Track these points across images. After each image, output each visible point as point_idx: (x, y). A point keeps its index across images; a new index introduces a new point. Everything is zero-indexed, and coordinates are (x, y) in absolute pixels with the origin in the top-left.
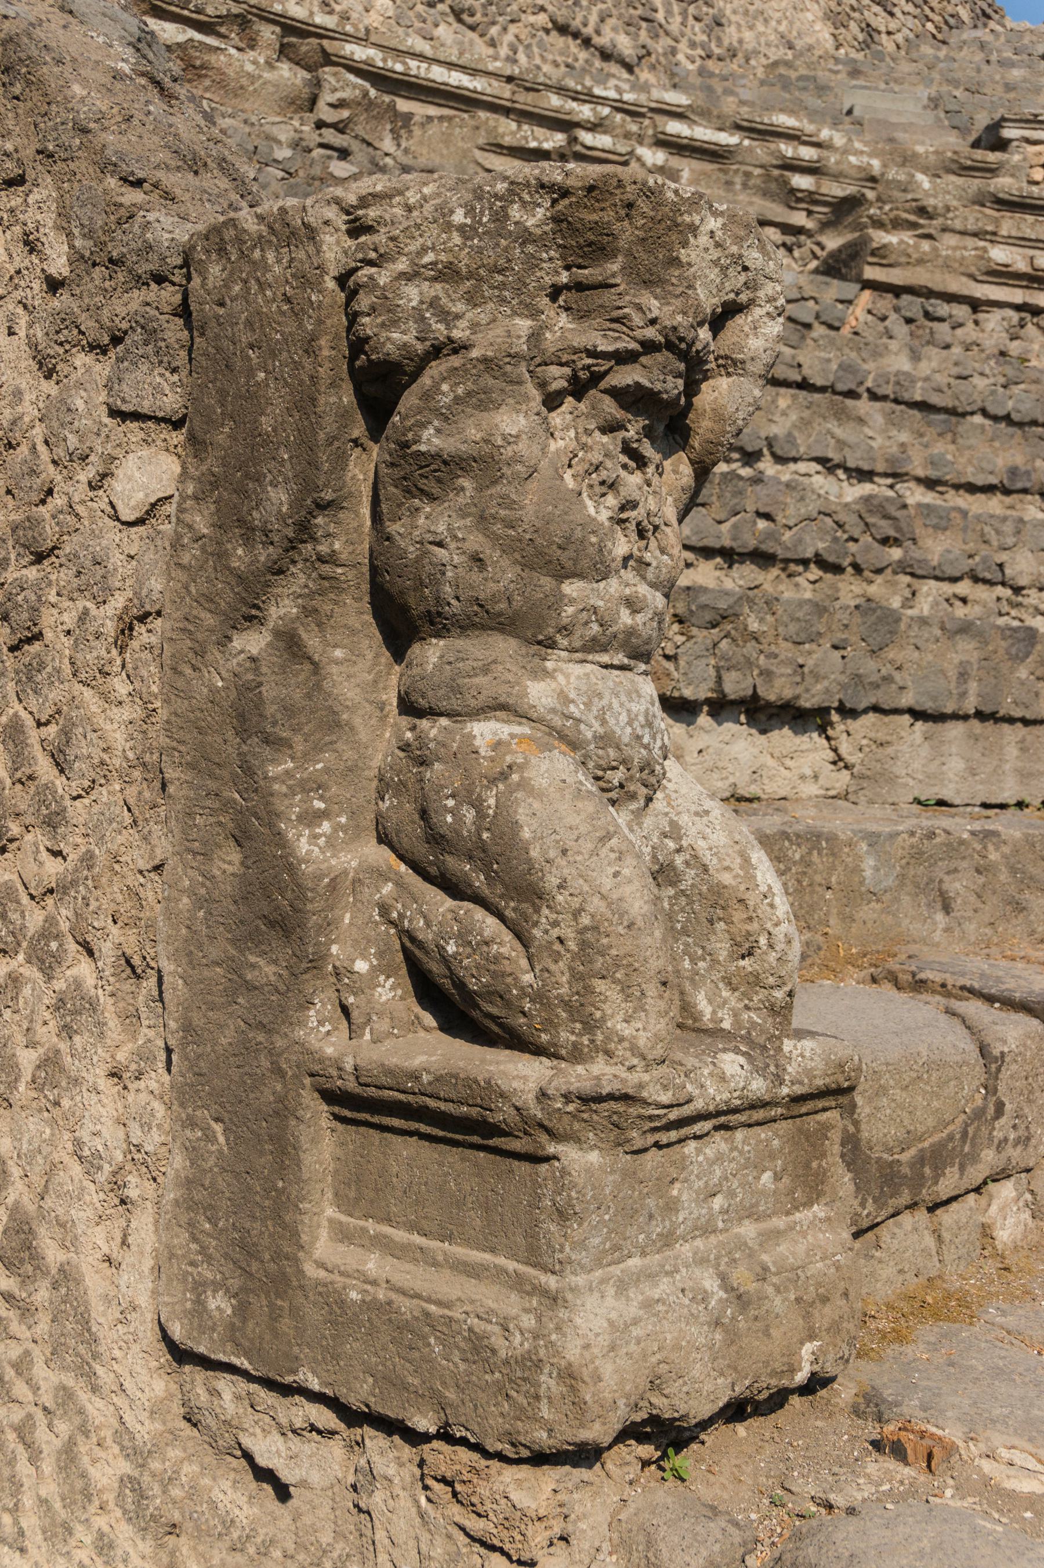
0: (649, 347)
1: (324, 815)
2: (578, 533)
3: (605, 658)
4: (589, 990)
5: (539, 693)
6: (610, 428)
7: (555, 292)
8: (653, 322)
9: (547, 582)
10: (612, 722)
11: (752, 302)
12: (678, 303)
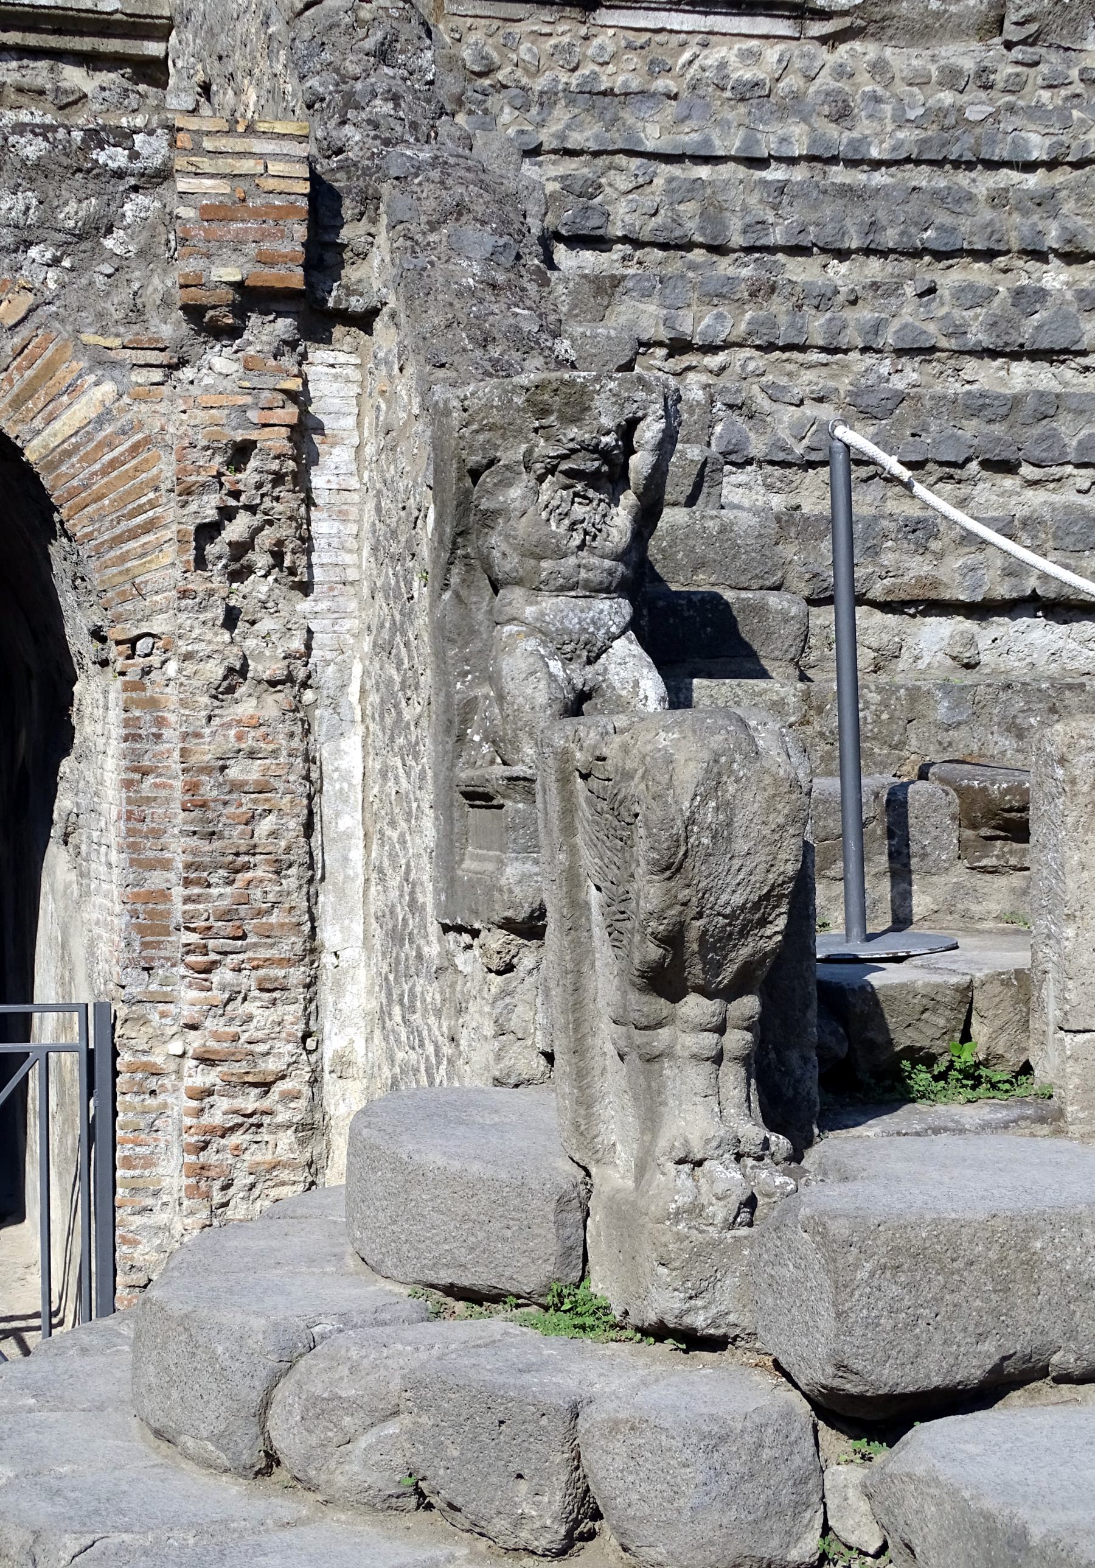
0: (573, 451)
1: (468, 672)
2: (544, 539)
3: (573, 593)
4: (517, 736)
5: (530, 612)
6: (566, 488)
7: (536, 430)
8: (572, 440)
9: (533, 562)
10: (567, 623)
11: (644, 417)
12: (588, 428)
